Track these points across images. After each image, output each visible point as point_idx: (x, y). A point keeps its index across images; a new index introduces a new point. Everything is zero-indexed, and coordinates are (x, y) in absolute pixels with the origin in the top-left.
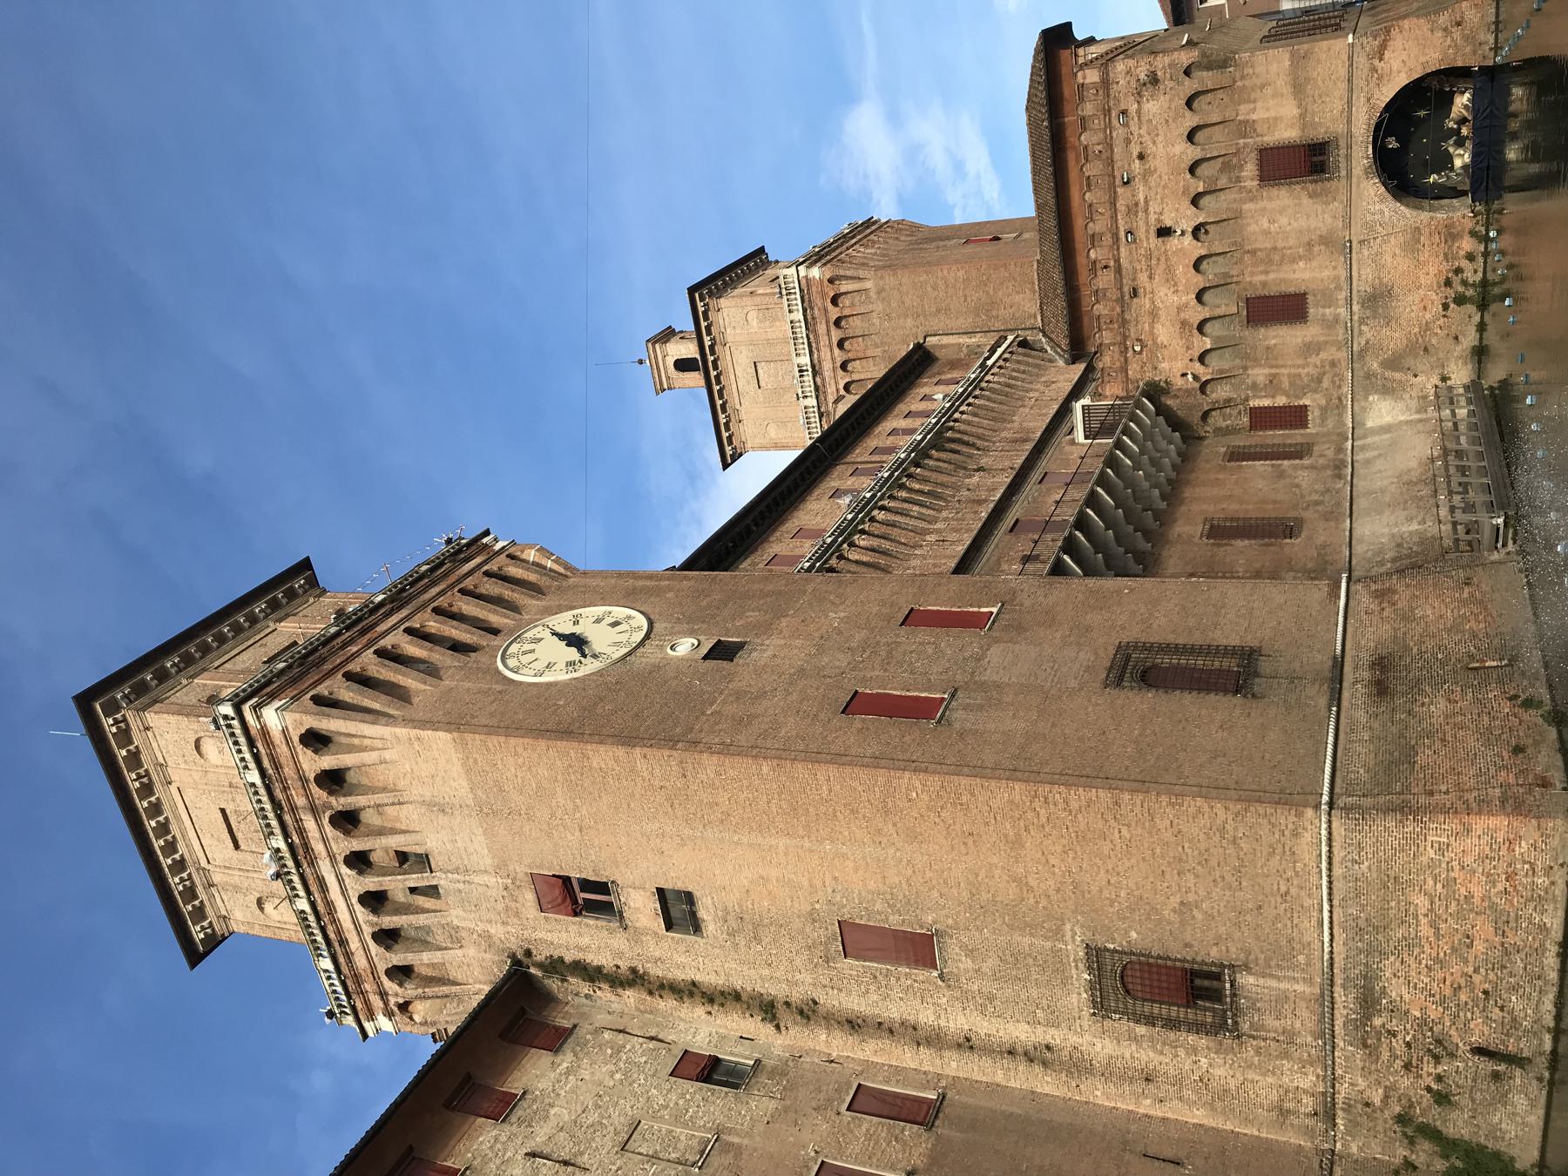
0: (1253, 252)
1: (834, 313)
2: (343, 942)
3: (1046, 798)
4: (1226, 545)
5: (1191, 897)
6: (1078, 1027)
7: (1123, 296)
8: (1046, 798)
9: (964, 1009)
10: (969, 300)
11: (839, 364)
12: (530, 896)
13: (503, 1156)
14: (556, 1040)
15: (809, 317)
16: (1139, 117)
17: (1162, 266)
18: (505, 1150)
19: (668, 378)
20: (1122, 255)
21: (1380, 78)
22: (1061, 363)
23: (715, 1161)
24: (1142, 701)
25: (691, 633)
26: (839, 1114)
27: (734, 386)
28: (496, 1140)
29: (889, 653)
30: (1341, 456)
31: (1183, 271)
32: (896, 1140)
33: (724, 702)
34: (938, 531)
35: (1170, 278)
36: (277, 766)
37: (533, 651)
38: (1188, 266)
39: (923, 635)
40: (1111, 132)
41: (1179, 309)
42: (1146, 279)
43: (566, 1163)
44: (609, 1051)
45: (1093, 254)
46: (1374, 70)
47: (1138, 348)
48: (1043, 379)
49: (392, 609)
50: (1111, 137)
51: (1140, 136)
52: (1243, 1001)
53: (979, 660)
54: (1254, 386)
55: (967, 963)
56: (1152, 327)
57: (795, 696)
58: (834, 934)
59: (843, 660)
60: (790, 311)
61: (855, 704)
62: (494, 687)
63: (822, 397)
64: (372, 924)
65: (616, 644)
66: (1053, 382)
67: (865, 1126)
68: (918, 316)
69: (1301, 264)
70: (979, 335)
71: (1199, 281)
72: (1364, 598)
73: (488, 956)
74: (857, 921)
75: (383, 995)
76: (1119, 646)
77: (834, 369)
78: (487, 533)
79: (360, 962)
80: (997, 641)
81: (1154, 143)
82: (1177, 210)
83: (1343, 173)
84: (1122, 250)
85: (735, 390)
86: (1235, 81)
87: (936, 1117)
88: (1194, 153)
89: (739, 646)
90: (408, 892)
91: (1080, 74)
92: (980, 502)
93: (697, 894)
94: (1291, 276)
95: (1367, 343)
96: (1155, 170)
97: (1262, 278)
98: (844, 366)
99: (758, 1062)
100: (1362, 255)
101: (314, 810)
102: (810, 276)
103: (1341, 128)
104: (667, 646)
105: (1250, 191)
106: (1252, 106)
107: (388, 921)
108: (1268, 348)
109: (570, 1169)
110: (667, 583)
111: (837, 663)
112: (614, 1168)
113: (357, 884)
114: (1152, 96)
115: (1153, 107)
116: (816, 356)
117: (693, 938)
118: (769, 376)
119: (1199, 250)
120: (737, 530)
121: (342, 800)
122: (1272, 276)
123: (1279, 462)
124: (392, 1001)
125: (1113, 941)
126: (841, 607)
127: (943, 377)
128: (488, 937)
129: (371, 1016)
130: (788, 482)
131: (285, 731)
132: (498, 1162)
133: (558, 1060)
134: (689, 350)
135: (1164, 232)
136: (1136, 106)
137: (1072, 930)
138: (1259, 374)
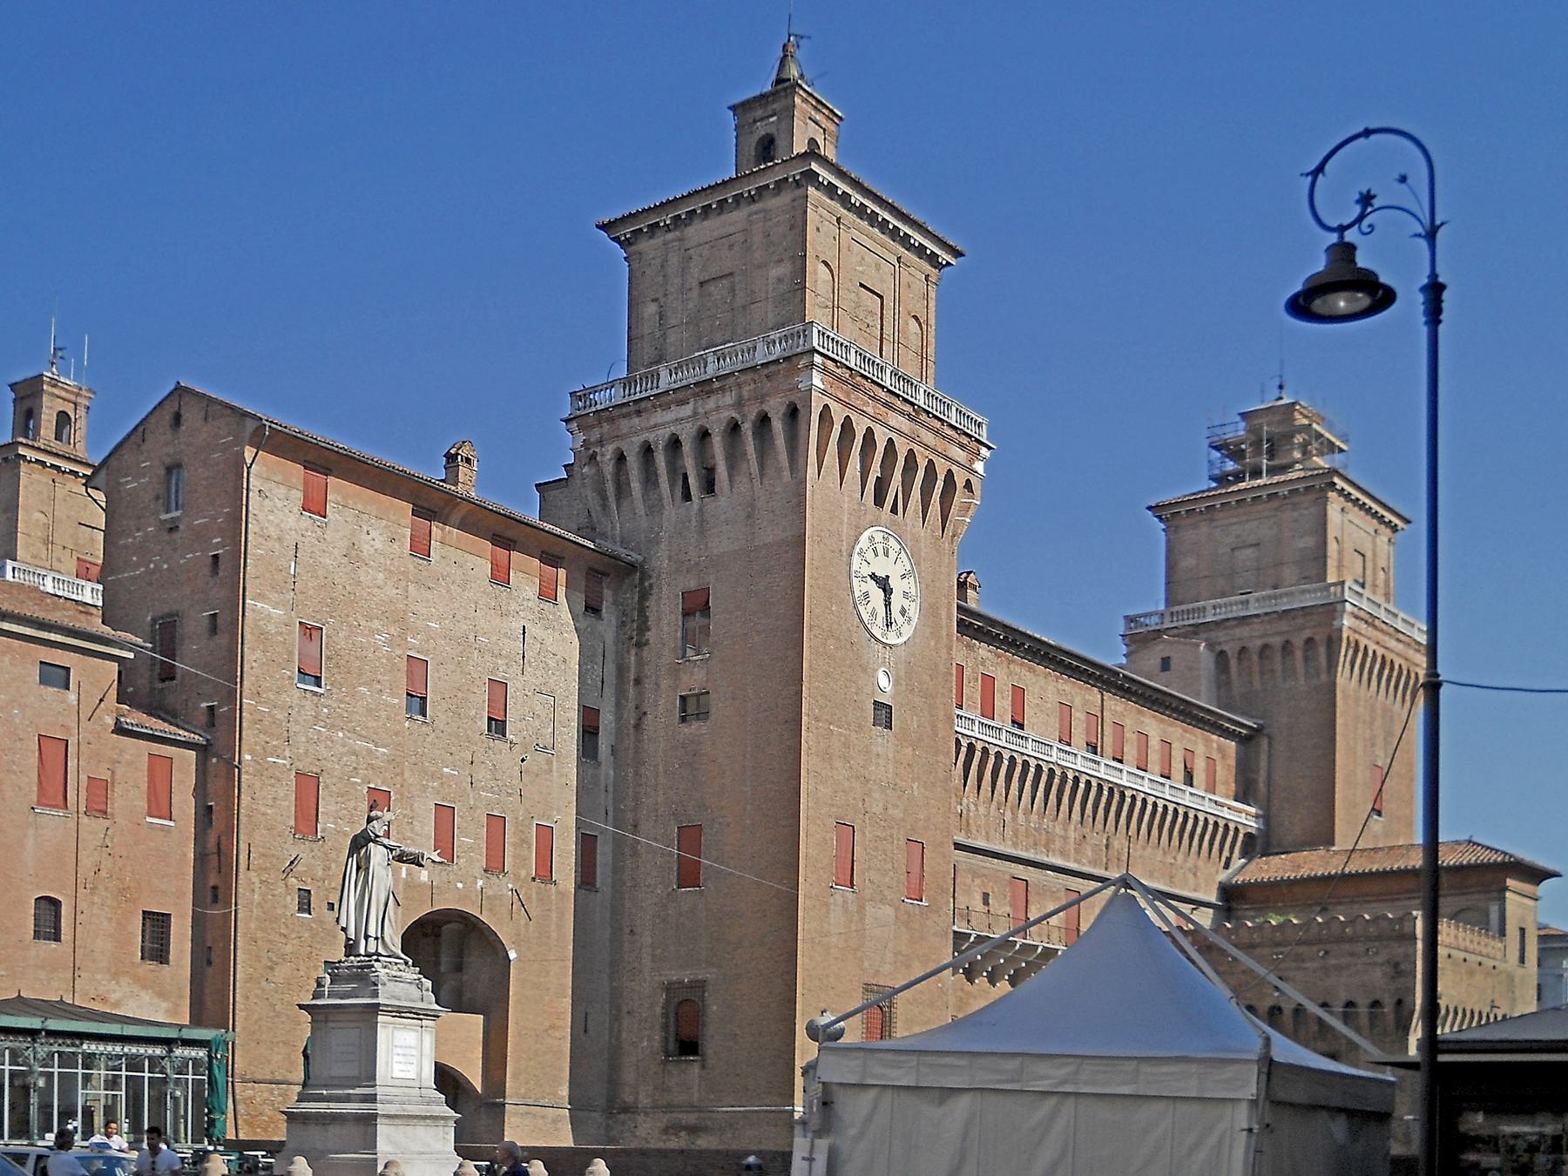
2: (639, 413)
12: (693, 584)
16: (1370, 964)
22: (1223, 876)
23: (542, 757)
25: (897, 683)
33: (841, 734)
34: (1014, 817)
37: (876, 555)
43: (524, 657)
48: (1200, 863)
50: (1357, 941)
51: (1356, 965)
57: (846, 784)
59: (877, 809)
61: (846, 830)
73: (643, 536)
90: (683, 471)
92: (1047, 846)
93: (708, 723)
104: (885, 666)
110: (945, 634)
112: (527, 692)
113: (687, 434)
115: (1377, 976)
121: (750, 433)
126: (923, 790)
132: (518, 609)
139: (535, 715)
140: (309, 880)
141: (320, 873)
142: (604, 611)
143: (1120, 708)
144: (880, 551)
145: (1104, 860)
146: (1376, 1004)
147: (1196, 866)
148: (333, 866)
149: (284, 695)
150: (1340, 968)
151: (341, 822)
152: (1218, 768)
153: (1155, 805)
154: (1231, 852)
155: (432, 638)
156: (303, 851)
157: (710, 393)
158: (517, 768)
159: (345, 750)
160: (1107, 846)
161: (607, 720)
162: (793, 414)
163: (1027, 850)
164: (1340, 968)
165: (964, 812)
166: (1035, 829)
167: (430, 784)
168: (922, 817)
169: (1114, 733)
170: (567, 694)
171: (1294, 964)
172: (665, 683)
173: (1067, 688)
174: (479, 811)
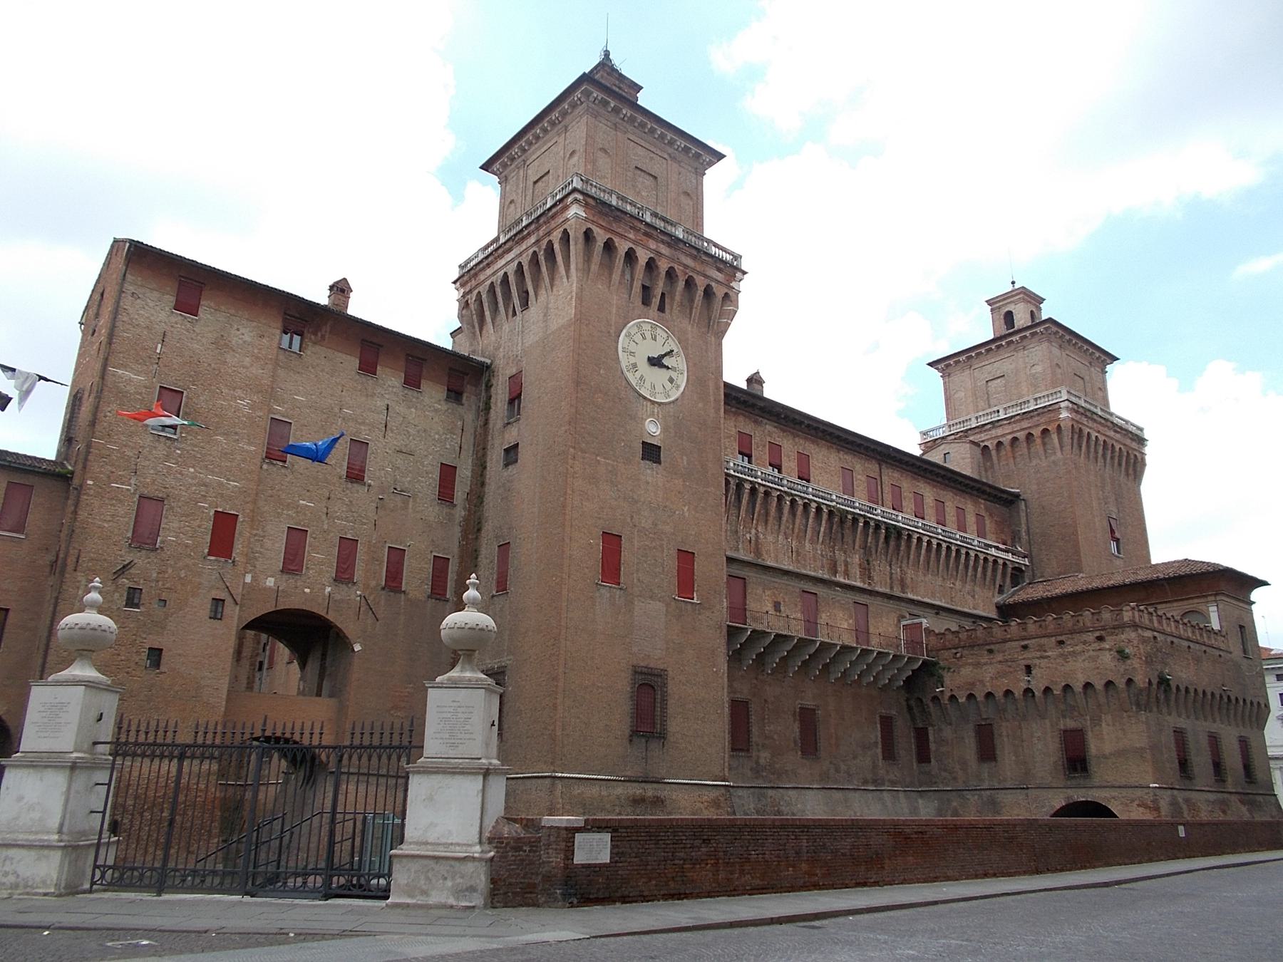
0: (1020, 728)
1: (1036, 432)
2: (488, 265)
5: (524, 715)
7: (987, 644)
10: (1052, 529)
11: (1001, 440)
12: (514, 371)
14: (455, 395)
15: (1032, 414)
17: (1008, 669)
18: (388, 394)
19: (999, 308)
20: (1013, 643)
21: (1127, 805)
22: (998, 599)
23: (398, 498)
24: (624, 684)
25: (665, 430)
26: (431, 552)
27: (987, 363)
28: (393, 387)
29: (654, 548)
30: (887, 783)
31: (1005, 683)
35: (1000, 675)
36: (553, 217)
37: (644, 338)
38: (1008, 686)
39: (672, 564)
40: (1090, 631)
41: (982, 682)
42: (999, 659)
45: (1013, 623)
46: (1132, 801)
47: (958, 655)
48: (977, 589)
49: (668, 243)
51: (1088, 651)
53: (651, 597)
54: (940, 730)
56: (969, 664)
60: (1036, 399)
62: (613, 327)
63: (977, 430)
64: (497, 281)
66: (973, 597)
67: (426, 566)
68: (1039, 493)
69: (1014, 758)
70: (1027, 537)
71: (999, 694)
72: (714, 794)
75: (470, 291)
77: (997, 437)
78: (744, 273)
79: (482, 277)
80: (668, 605)
81: (1084, 660)
82: (1042, 677)
83: (1069, 783)
84: (1017, 643)
85: (983, 364)
86: (1126, 712)
87: (436, 599)
88: (1078, 687)
89: (658, 461)
91: (1128, 608)
94: (1006, 752)
95: (968, 799)
96: (1067, 662)
97: (1004, 733)
98: (1000, 444)
99: (456, 505)
100: (1020, 795)
101: (538, 241)
102: (1062, 411)
103: (1096, 780)
105: (1057, 725)
106: (1111, 723)
107: (498, 290)
108: (963, 738)
109: (384, 429)
111: (643, 521)
112: (387, 450)
114: (1114, 657)
115: (1107, 659)
116: (1005, 422)
117: (502, 464)
118: (995, 387)
119: (1018, 693)
120: (797, 417)
121: (543, 258)
122: (1005, 739)
123: (880, 746)
124: (469, 297)
127: (986, 518)
128: (497, 349)
129: (462, 285)
130: (851, 438)
131: (567, 219)
132: (383, 392)
133: (442, 402)
134: (1021, 319)
135: (1028, 669)
136: (1108, 647)
138: (948, 732)
139: (396, 468)
140: (142, 581)
141: (155, 575)
142: (464, 398)
143: (896, 475)
144: (648, 335)
145: (888, 581)
146: (1109, 684)
147: (974, 591)
148: (170, 571)
150: (1074, 653)
152: (988, 522)
153: (929, 543)
154: (1004, 581)
155: (297, 407)
156: (141, 560)
157: (524, 239)
158: (375, 505)
160: (891, 574)
161: (465, 473)
162: (566, 237)
163: (815, 571)
164: (1074, 653)
165: (753, 539)
167: (285, 512)
168: (693, 533)
169: (893, 492)
170: (425, 453)
171: (1038, 654)
172: (497, 442)
173: (848, 457)
174: (332, 534)
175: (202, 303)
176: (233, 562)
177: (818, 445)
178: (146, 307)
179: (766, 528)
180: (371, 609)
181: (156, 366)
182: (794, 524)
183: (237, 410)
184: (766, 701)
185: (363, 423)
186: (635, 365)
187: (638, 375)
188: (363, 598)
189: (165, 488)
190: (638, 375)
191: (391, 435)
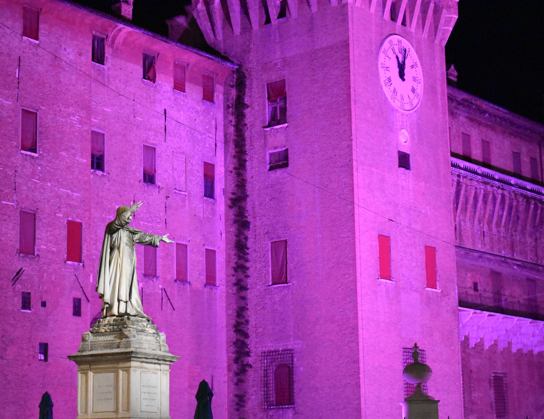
3: (353, 333)
4: (491, 386)
6: (258, 346)
8: (353, 333)
9: (257, 296)
13: (162, 99)
32: (199, 274)
43: (165, 129)
44: (208, 127)
52: (281, 412)
53: (411, 289)
55: (277, 298)
58: (280, 237)
65: (402, 98)
74: (287, 248)
76: (423, 351)
80: (421, 295)
112: (168, 153)
125: (298, 360)
133: (200, 104)
137: (299, 344)
149: (12, 159)
151: (50, 244)
159: (52, 194)
166: (504, 237)
175: (41, 26)
176: (83, 265)
177: (495, 131)
178: (6, 35)
179: (466, 216)
180: (169, 300)
181: (17, 90)
182: (485, 209)
183: (72, 126)
184: (471, 371)
185: (150, 129)
186: (389, 80)
187: (392, 88)
188: (164, 292)
189: (35, 202)
190: (392, 88)
191: (169, 138)
